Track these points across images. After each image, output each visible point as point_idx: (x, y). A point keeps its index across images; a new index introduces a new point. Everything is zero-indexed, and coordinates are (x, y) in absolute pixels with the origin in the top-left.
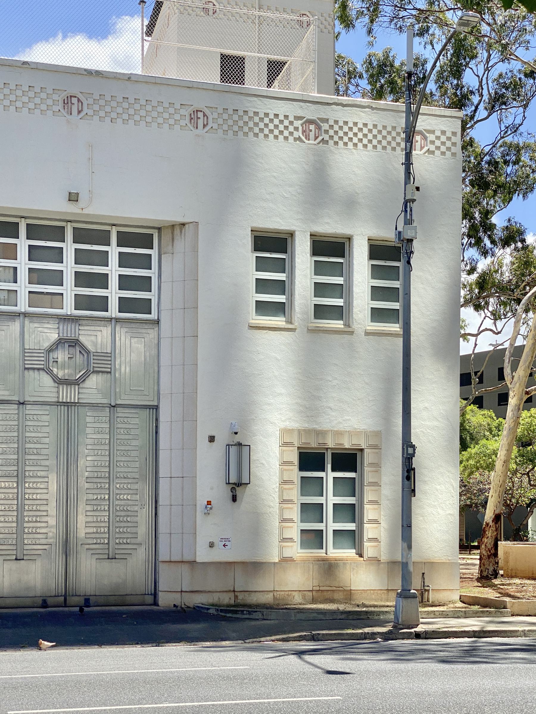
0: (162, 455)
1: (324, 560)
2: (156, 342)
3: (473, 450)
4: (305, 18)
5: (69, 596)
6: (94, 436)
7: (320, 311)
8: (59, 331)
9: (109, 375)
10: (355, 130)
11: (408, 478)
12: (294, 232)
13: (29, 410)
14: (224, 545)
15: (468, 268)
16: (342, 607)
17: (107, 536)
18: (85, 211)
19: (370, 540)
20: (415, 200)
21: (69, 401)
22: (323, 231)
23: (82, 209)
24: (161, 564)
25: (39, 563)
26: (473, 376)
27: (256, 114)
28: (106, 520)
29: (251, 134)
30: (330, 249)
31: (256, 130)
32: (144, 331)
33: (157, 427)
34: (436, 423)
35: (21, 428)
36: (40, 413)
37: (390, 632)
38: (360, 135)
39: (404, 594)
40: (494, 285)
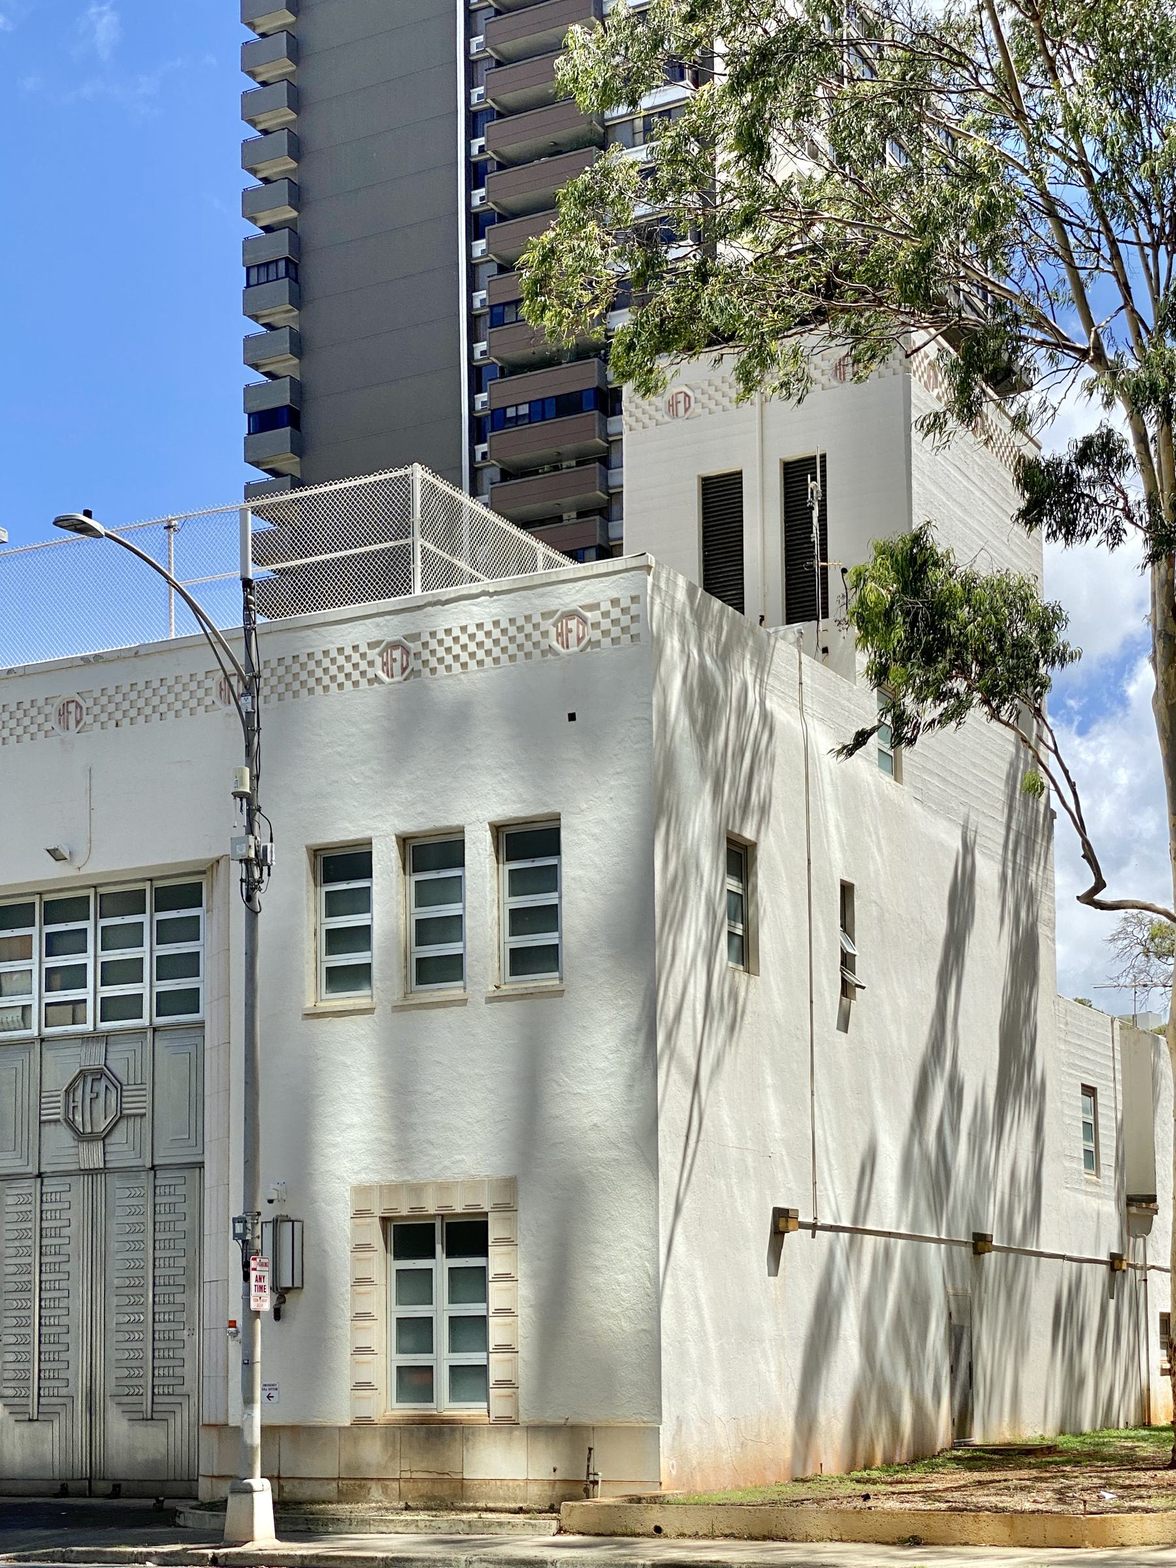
12: (397, 837)
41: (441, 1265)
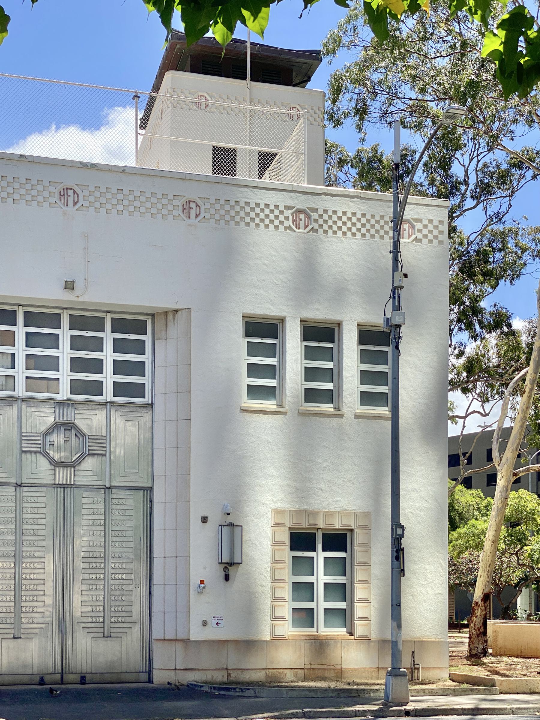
0: (156, 535)
1: (315, 639)
2: (150, 425)
3: (462, 530)
4: (295, 112)
5: (66, 673)
6: (89, 517)
7: (311, 395)
8: (55, 415)
9: (104, 457)
10: (344, 219)
11: (397, 558)
12: (285, 318)
13: (27, 491)
14: (217, 624)
15: (457, 351)
16: (333, 685)
17: (102, 614)
18: (81, 299)
19: (361, 618)
20: (403, 287)
21: (65, 483)
22: (313, 317)
23: (78, 297)
24: (155, 642)
25: (36, 641)
26: (462, 458)
27: (247, 204)
28: (102, 599)
29: (242, 224)
30: (321, 335)
31: (248, 219)
32: (139, 415)
33: (151, 508)
34: (424, 504)
35: (19, 510)
36: (38, 495)
37: (380, 710)
38: (349, 224)
39: (394, 673)
40: (481, 369)
41: (320, 556)
